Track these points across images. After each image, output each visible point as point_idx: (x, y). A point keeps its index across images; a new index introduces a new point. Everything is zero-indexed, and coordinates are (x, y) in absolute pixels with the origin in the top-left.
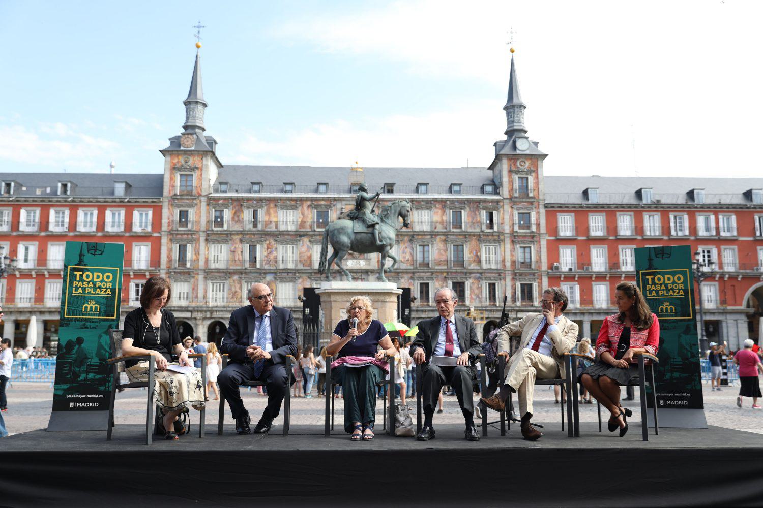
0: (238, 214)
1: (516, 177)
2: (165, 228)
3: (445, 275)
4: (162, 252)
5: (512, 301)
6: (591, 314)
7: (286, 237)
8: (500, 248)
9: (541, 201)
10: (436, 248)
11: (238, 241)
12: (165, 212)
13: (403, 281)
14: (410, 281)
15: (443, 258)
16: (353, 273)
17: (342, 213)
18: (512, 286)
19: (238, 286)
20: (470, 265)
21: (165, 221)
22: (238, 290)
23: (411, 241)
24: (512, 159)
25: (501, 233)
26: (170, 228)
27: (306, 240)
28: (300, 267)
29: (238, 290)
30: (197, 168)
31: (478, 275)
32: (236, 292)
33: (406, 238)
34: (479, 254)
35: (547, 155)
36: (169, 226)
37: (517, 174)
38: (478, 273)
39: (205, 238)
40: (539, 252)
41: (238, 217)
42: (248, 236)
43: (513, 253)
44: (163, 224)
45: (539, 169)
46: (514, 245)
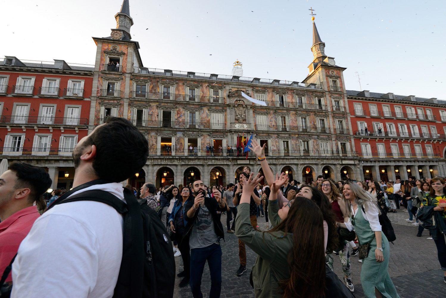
0: (155, 89)
1: (330, 80)
2: (94, 94)
3: (297, 136)
4: (91, 112)
5: (337, 153)
6: (379, 161)
7: (191, 106)
8: (327, 120)
9: (345, 95)
10: (290, 119)
11: (155, 107)
12: (95, 83)
14: (276, 139)
15: (295, 125)
16: (240, 132)
17: (230, 92)
18: (336, 144)
19: (154, 140)
20: (311, 130)
21: (94, 89)
22: (155, 143)
23: (275, 113)
24: (327, 69)
25: (327, 111)
26: (99, 95)
27: (205, 109)
28: (202, 127)
29: (155, 143)
30: (124, 54)
31: (316, 137)
32: (153, 145)
34: (315, 123)
35: (345, 69)
36: (98, 93)
37: (331, 78)
38: (316, 135)
39: (128, 103)
40: (347, 124)
41: (155, 90)
42: (163, 104)
43: (334, 124)
44: (93, 92)
45: (342, 77)
46: (334, 119)
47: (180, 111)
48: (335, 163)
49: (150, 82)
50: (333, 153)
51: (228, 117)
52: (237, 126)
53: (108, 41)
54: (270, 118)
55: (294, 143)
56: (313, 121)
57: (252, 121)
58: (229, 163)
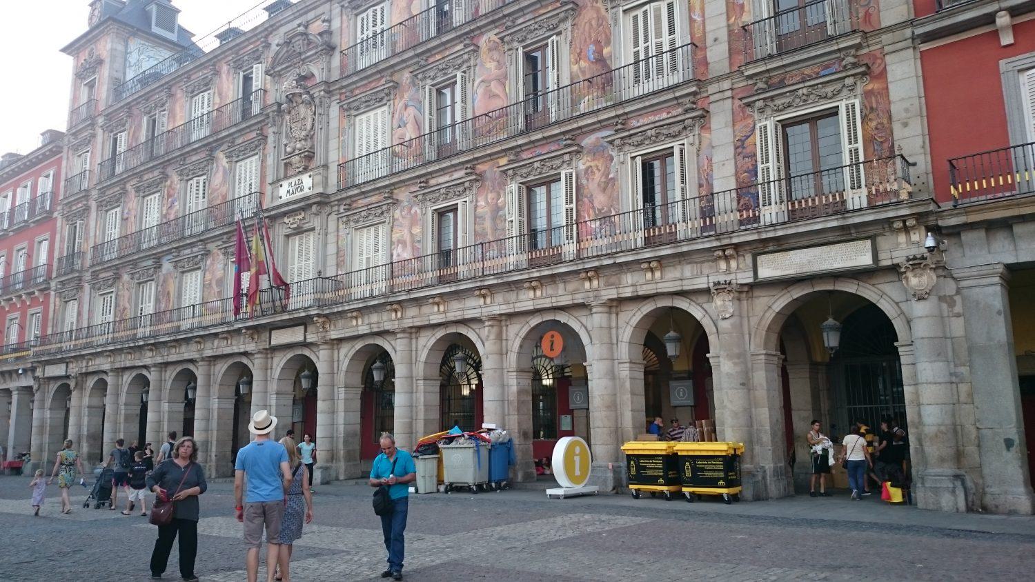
13: (397, 214)
20: (575, 103)
29: (127, 305)
33: (406, 77)
34: (605, 51)
38: (602, 125)
47: (173, 186)
48: (701, 283)
49: (129, 120)
50: (707, 212)
51: (270, 161)
52: (285, 192)
53: (94, 34)
54: (400, 113)
55: (487, 209)
56: (597, 42)
57: (334, 157)
58: (251, 347)
